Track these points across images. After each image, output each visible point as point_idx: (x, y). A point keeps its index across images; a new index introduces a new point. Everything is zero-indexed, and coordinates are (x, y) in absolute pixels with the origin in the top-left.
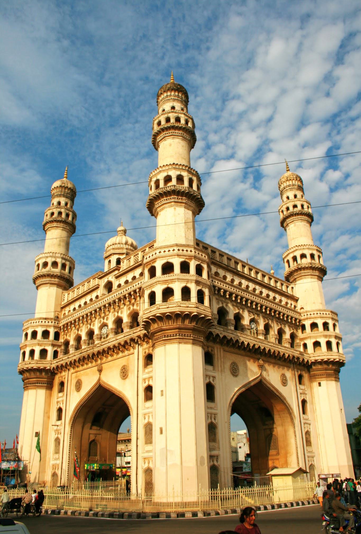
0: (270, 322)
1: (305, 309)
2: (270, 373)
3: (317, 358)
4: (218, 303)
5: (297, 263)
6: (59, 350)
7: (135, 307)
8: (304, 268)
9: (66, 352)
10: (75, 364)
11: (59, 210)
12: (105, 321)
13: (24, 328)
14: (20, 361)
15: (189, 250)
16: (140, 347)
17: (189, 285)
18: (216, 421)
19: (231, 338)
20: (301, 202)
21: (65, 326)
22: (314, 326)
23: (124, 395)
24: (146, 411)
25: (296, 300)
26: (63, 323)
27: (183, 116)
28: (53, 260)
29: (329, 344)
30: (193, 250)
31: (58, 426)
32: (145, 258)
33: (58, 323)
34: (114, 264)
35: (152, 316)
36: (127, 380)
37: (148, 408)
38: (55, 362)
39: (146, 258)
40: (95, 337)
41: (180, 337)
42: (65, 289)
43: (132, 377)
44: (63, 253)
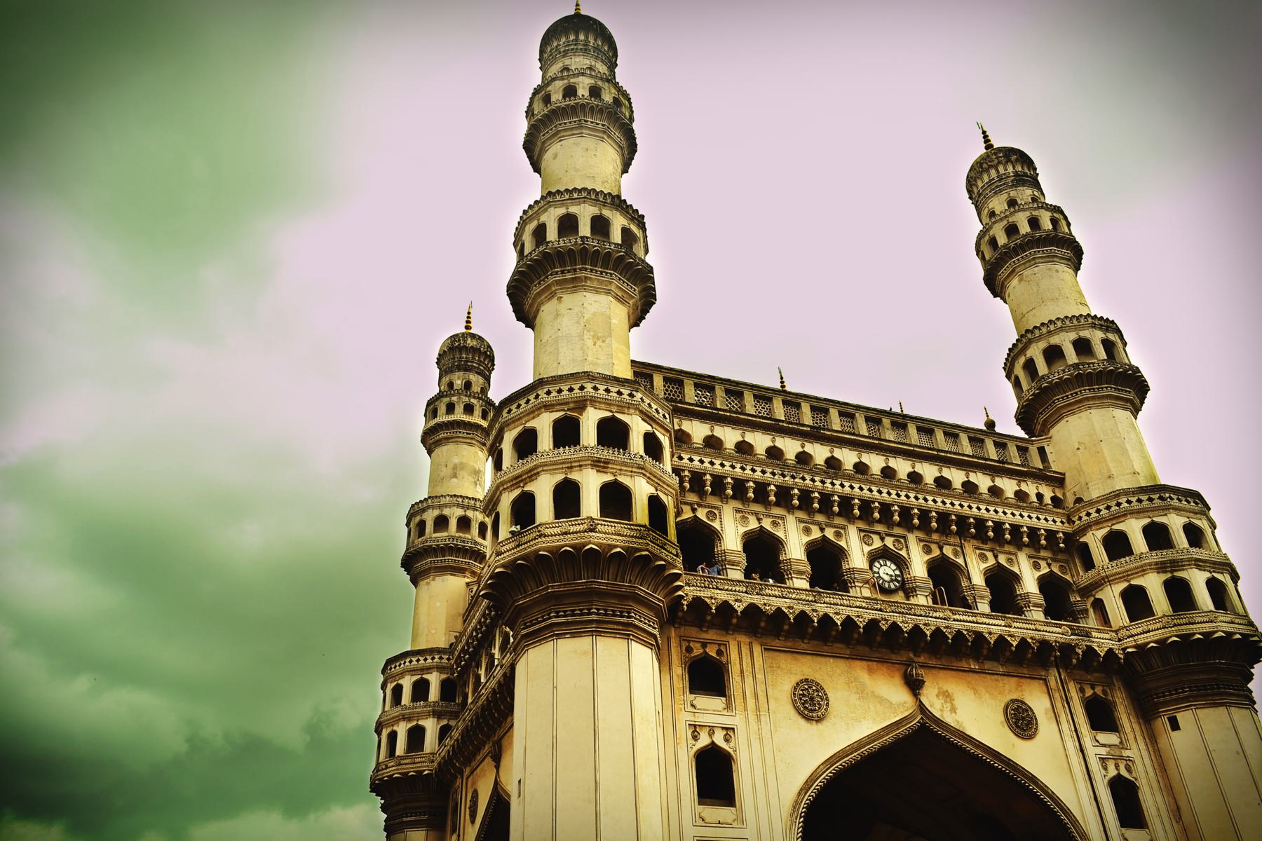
2: (955, 703)
3: (1142, 639)
6: (453, 723)
8: (1062, 385)
15: (576, 387)
17: (574, 476)
19: (779, 609)
22: (1117, 545)
25: (1058, 481)
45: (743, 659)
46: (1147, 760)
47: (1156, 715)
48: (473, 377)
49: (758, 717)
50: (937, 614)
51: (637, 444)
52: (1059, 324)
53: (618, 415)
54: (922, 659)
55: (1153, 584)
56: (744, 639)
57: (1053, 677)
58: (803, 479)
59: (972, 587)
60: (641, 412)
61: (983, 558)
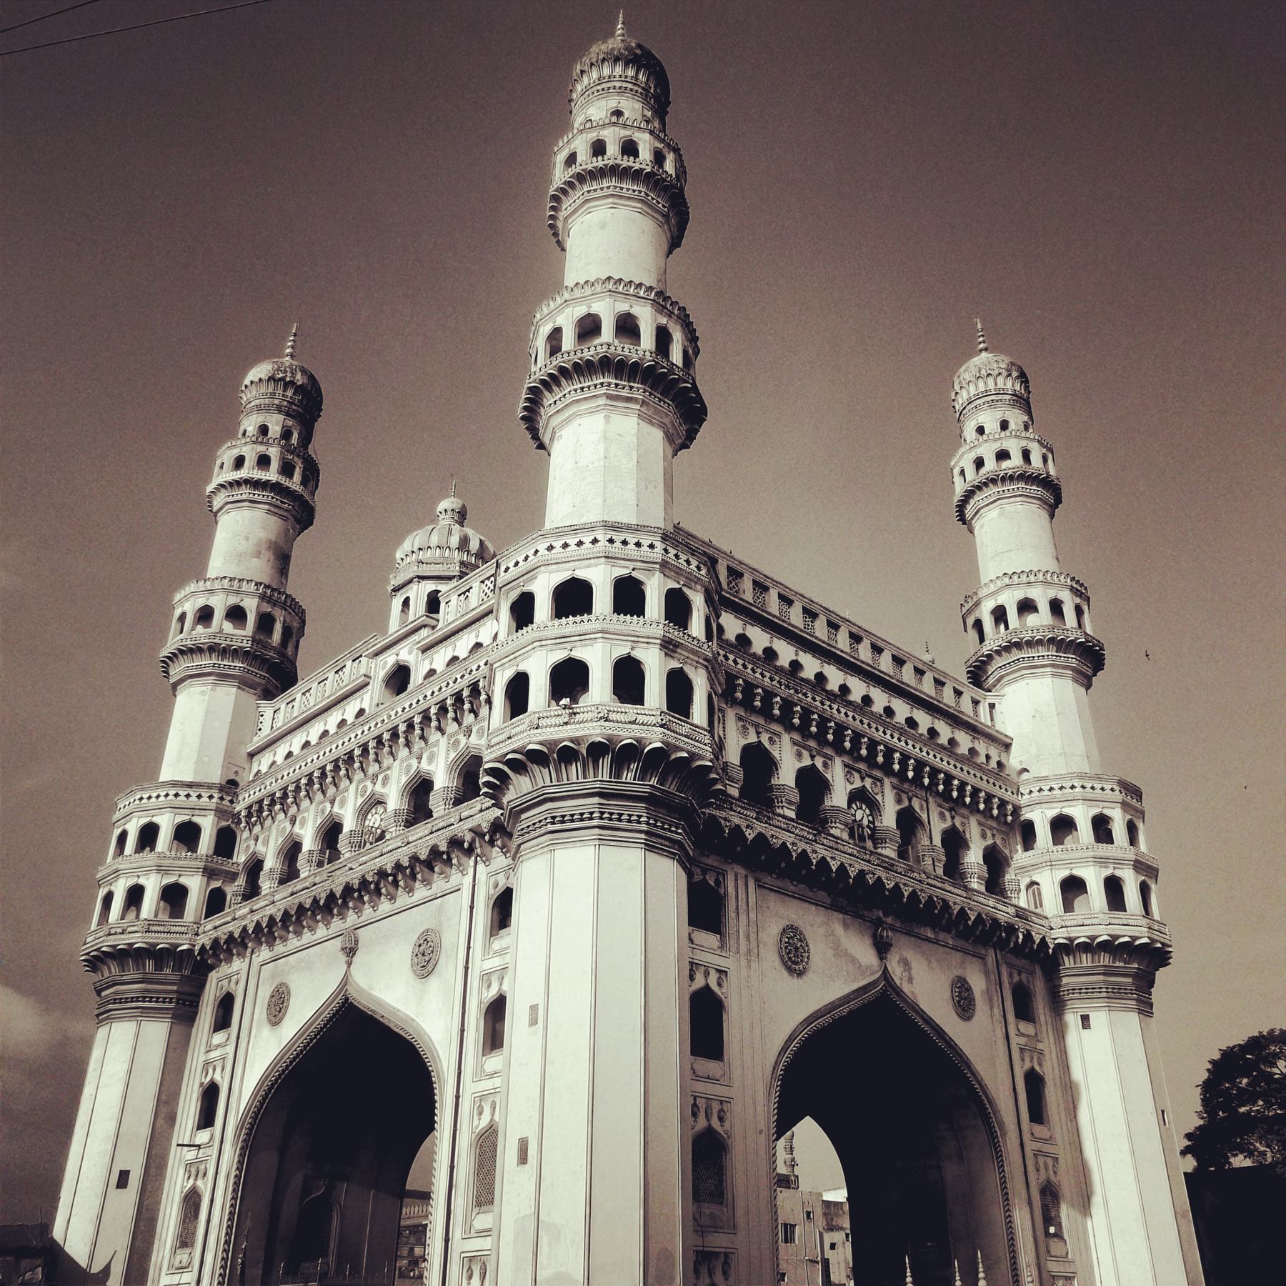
0: (916, 804)
1: (1034, 772)
2: (914, 972)
5: (1007, 628)
7: (473, 739)
9: (252, 891)
10: (271, 933)
12: (378, 788)
13: (117, 815)
14: (94, 926)
15: (645, 543)
16: (481, 866)
17: (638, 654)
19: (784, 844)
20: (1024, 443)
21: (255, 808)
23: (419, 1029)
24: (487, 1085)
26: (248, 802)
27: (647, 136)
28: (233, 600)
29: (1113, 887)
30: (659, 546)
31: (199, 1146)
32: (503, 568)
33: (232, 802)
34: (418, 607)
35: (514, 751)
36: (434, 981)
37: (492, 1075)
39: (507, 569)
40: (343, 843)
41: (606, 823)
42: (268, 694)
43: (450, 969)
44: (266, 580)
45: (739, 890)
49: (749, 961)
51: (697, 626)
52: (1041, 577)
53: (685, 589)
54: (889, 920)
56: (741, 871)
58: (805, 695)
59: (932, 848)
61: (942, 816)
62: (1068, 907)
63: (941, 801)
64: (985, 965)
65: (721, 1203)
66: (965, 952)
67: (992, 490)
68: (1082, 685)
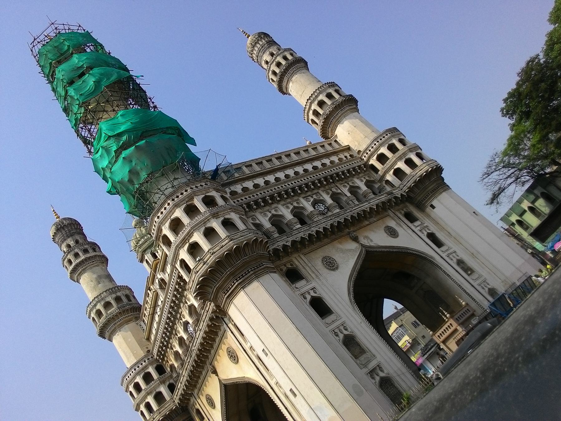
4: (265, 215)
6: (172, 381)
11: (73, 253)
12: (184, 320)
17: (208, 225)
18: (349, 330)
19: (301, 237)
22: (382, 158)
25: (348, 149)
38: (175, 397)
40: (187, 343)
45: (300, 262)
46: (431, 224)
47: (426, 207)
48: (78, 237)
50: (349, 211)
51: (220, 202)
54: (352, 230)
55: (401, 165)
56: (296, 255)
57: (390, 212)
60: (214, 189)
61: (345, 186)
62: (401, 180)
63: (341, 182)
64: (391, 217)
65: (365, 352)
66: (382, 218)
67: (285, 80)
68: (356, 112)
